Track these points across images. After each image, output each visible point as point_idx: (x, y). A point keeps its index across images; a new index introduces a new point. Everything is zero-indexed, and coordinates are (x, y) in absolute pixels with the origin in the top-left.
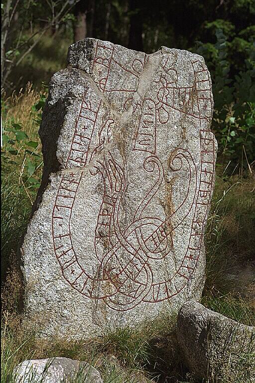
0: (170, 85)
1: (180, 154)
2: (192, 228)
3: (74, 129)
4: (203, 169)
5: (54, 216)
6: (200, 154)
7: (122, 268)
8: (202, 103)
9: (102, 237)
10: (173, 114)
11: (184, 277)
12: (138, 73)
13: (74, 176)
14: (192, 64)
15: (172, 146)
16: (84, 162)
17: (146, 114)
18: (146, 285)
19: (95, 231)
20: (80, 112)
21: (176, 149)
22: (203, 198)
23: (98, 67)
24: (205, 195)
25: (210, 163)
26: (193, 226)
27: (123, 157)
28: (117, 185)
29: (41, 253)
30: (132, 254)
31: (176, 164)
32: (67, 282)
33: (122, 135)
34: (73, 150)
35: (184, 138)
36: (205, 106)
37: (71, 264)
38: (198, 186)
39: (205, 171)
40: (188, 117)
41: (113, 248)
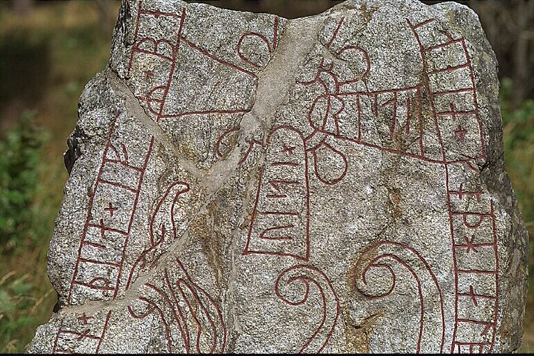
0: (347, 88)
1: (385, 255)
3: (86, 212)
4: (464, 286)
6: (450, 253)
8: (449, 124)
10: (361, 159)
12: (252, 65)
13: (88, 321)
14: (413, 28)
15: (358, 237)
16: (112, 289)
17: (276, 164)
20: (101, 171)
21: (374, 244)
23: (144, 61)
25: (485, 272)
27: (215, 271)
28: (203, 339)
31: (376, 279)
33: (213, 219)
34: (84, 260)
35: (398, 213)
36: (461, 131)
38: (449, 331)
39: (471, 293)
40: (405, 163)
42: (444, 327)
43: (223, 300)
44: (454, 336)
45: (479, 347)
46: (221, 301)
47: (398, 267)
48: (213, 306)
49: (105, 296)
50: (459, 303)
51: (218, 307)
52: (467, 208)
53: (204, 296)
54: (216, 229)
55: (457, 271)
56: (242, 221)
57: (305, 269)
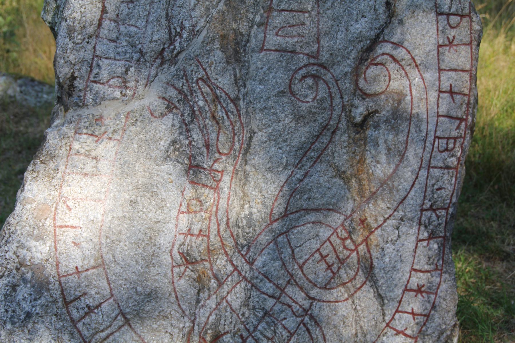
1: (383, 54)
2: (420, 224)
4: (445, 86)
5: (58, 223)
6: (435, 52)
7: (248, 330)
9: (193, 263)
15: (360, 38)
19: (171, 251)
22: (445, 154)
24: (451, 146)
26: (423, 219)
29: (29, 315)
37: (112, 334)
38: (431, 127)
41: (220, 284)
42: (428, 123)
43: (242, 99)
44: (436, 131)
45: (453, 141)
46: (239, 99)
47: (392, 66)
48: (232, 105)
49: (124, 96)
50: (440, 100)
51: (235, 105)
53: (223, 95)
54: (234, 26)
55: (440, 70)
56: (258, 19)
57: (315, 68)
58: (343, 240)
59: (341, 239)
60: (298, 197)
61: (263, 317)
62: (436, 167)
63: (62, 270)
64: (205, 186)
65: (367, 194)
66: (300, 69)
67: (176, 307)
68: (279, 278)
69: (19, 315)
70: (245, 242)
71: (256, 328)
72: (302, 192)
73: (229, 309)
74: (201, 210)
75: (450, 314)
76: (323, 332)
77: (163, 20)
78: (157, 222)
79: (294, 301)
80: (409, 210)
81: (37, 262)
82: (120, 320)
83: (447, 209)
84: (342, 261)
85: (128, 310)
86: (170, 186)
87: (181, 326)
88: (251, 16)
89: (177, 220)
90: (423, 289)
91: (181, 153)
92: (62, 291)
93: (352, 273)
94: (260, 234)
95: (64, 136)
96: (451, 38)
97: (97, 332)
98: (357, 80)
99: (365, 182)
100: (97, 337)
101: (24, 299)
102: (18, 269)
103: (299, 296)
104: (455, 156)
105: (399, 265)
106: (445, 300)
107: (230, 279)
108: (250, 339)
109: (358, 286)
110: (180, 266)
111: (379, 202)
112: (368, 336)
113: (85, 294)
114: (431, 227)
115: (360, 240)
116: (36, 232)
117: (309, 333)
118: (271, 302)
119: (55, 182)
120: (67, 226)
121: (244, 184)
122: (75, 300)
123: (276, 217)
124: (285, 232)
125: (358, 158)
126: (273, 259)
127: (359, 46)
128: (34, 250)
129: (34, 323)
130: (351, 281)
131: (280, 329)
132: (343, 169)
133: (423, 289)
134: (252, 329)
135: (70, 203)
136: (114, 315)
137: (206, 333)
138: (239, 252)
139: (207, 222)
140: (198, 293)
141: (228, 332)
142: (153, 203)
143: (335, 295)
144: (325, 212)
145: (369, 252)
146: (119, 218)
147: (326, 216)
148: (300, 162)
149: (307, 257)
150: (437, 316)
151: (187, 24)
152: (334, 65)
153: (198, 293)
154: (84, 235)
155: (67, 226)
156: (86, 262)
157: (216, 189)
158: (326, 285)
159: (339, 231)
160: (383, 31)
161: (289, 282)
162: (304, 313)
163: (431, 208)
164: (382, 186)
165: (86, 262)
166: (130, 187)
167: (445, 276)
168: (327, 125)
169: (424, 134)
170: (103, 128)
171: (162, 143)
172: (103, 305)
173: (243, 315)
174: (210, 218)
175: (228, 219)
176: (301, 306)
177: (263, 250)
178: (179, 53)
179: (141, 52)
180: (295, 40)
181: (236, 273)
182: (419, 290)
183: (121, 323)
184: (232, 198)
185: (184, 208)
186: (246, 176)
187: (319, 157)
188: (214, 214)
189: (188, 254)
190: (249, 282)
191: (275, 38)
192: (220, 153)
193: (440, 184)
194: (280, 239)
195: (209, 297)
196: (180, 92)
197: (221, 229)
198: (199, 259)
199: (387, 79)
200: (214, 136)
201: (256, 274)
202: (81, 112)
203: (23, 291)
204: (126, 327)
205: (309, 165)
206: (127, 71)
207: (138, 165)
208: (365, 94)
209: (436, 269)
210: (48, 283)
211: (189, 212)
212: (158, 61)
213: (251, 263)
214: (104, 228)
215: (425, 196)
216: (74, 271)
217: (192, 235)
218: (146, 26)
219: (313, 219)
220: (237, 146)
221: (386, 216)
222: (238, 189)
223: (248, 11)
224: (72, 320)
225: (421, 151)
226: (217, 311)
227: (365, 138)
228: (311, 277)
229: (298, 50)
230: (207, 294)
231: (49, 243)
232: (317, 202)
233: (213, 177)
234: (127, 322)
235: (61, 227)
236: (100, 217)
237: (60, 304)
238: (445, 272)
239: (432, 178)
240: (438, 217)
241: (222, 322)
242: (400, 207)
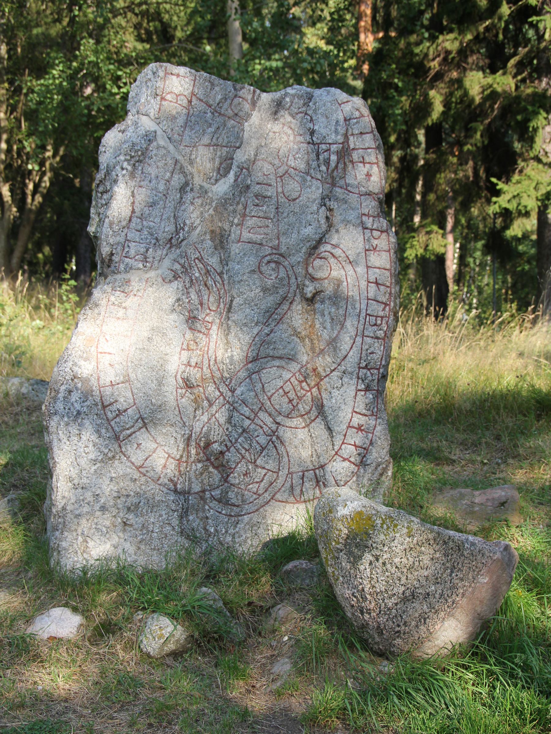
1: (325, 251)
2: (358, 378)
4: (372, 279)
5: (100, 350)
6: (364, 254)
7: (231, 441)
9: (191, 387)
11: (350, 462)
15: (307, 239)
17: (258, 184)
18: (278, 473)
19: (176, 376)
22: (375, 328)
29: (79, 413)
30: (248, 418)
32: (129, 464)
37: (134, 432)
38: (363, 306)
41: (211, 405)
44: (367, 310)
47: (332, 260)
50: (369, 288)
51: (221, 277)
52: (373, 225)
53: (212, 270)
54: (220, 224)
55: (368, 267)
56: (236, 221)
57: (277, 256)
58: (301, 382)
59: (299, 381)
60: (266, 346)
61: (242, 433)
62: (368, 337)
63: (102, 382)
64: (200, 332)
65: (317, 350)
66: (266, 256)
67: (179, 419)
68: (253, 405)
69: (73, 412)
70: (228, 376)
71: (237, 440)
72: (269, 343)
73: (217, 424)
74: (197, 349)
75: (384, 451)
76: (286, 450)
77: (172, 219)
78: (166, 355)
79: (265, 424)
80: (349, 366)
81: (85, 376)
82: (140, 424)
83: (378, 369)
84: (300, 398)
85: (145, 416)
86: (175, 330)
87: (183, 433)
88: (231, 219)
89: (180, 354)
90: (362, 428)
91: (183, 308)
92: (101, 397)
93: (308, 408)
94: (239, 371)
95: (105, 292)
96: (375, 246)
97: (124, 429)
98: (307, 268)
99: (316, 342)
100: (124, 433)
101: (76, 401)
102: (72, 380)
103: (268, 420)
104: (382, 330)
105: (343, 407)
106: (380, 439)
107: (217, 401)
108: (233, 448)
109: (313, 418)
110: (182, 388)
111: (327, 357)
112: (321, 458)
113: (116, 401)
114: (367, 381)
115: (313, 384)
116: (85, 355)
117: (276, 449)
118: (247, 422)
119: (98, 322)
120: (105, 353)
121: (228, 334)
122: (110, 405)
123: (251, 359)
124: (257, 372)
125: (310, 323)
126: (248, 390)
127: (308, 245)
128: (83, 368)
129: (82, 419)
130: (307, 414)
131: (255, 444)
132: (299, 330)
133: (362, 428)
134: (234, 441)
135: (108, 337)
136: (136, 418)
137: (200, 440)
138: (224, 382)
139: (201, 357)
140: (195, 411)
141: (216, 442)
142: (164, 341)
143: (295, 423)
144: (286, 360)
145: (320, 394)
146: (140, 349)
147: (287, 363)
148: (267, 321)
149: (274, 391)
150: (374, 450)
151: (188, 222)
152: (290, 255)
153: (195, 411)
154: (117, 359)
155: (105, 353)
156: (118, 378)
157: (207, 335)
158: (288, 414)
159: (297, 375)
160: (324, 236)
161: (260, 409)
162: (272, 434)
163: (366, 367)
164: (328, 345)
165: (118, 378)
166: (148, 329)
167: (379, 421)
168: (286, 297)
169: (358, 311)
170: (131, 288)
171: (170, 300)
172: (129, 410)
173: (227, 429)
174: (203, 356)
175: (216, 357)
176: (270, 428)
177: (241, 383)
178: (182, 241)
179: (157, 239)
180: (262, 236)
181: (222, 398)
182: (359, 428)
183: (140, 425)
184: (219, 342)
185: (185, 347)
186: (229, 328)
187: (281, 319)
188: (206, 352)
189: (188, 380)
190: (232, 405)
191: (248, 234)
192: (210, 310)
193: (372, 349)
194: (253, 376)
195: (203, 413)
196: (183, 267)
197: (211, 363)
198: (195, 384)
199: (329, 269)
200: (206, 297)
201: (237, 400)
202: (116, 276)
203: (75, 397)
204: (144, 429)
205: (274, 324)
206: (147, 250)
207: (153, 314)
208: (313, 278)
209: (373, 415)
210: (92, 391)
211: (188, 350)
212: (168, 246)
213: (233, 391)
214: (130, 355)
215: (361, 358)
216: (110, 384)
217: (190, 366)
218: (160, 223)
219: (277, 364)
220: (222, 306)
221: (332, 368)
222: (223, 337)
223: (229, 215)
224: (108, 420)
225: (357, 323)
226: (208, 425)
227: (314, 310)
228: (277, 407)
229: (264, 243)
230: (201, 411)
231: (94, 363)
232: (281, 352)
233: (206, 326)
234: (145, 425)
235: (101, 353)
236: (127, 348)
237: (100, 407)
238: (380, 418)
239: (366, 344)
240: (372, 374)
241: (212, 433)
242: (342, 363)
